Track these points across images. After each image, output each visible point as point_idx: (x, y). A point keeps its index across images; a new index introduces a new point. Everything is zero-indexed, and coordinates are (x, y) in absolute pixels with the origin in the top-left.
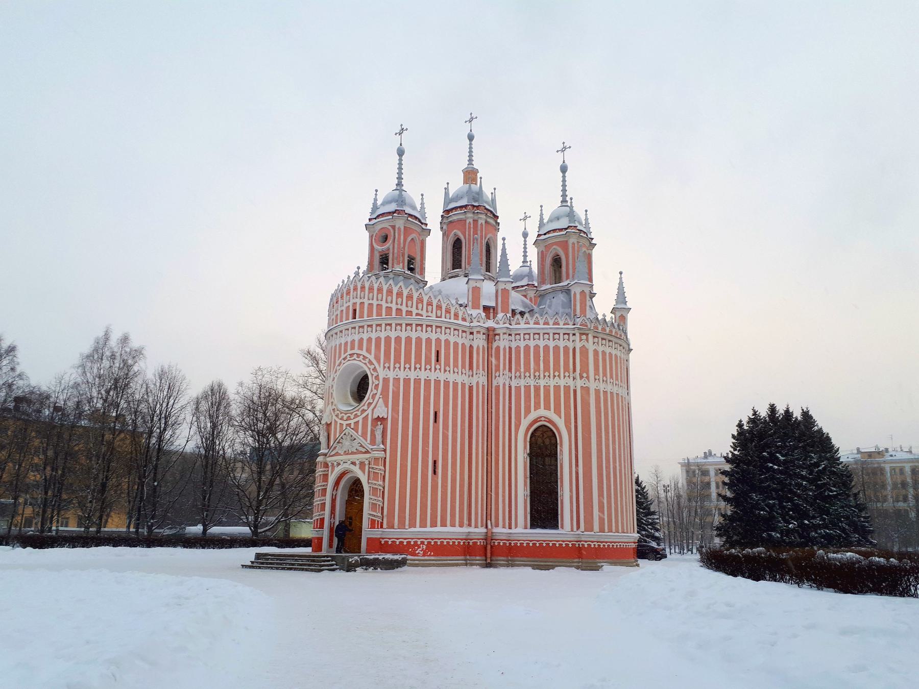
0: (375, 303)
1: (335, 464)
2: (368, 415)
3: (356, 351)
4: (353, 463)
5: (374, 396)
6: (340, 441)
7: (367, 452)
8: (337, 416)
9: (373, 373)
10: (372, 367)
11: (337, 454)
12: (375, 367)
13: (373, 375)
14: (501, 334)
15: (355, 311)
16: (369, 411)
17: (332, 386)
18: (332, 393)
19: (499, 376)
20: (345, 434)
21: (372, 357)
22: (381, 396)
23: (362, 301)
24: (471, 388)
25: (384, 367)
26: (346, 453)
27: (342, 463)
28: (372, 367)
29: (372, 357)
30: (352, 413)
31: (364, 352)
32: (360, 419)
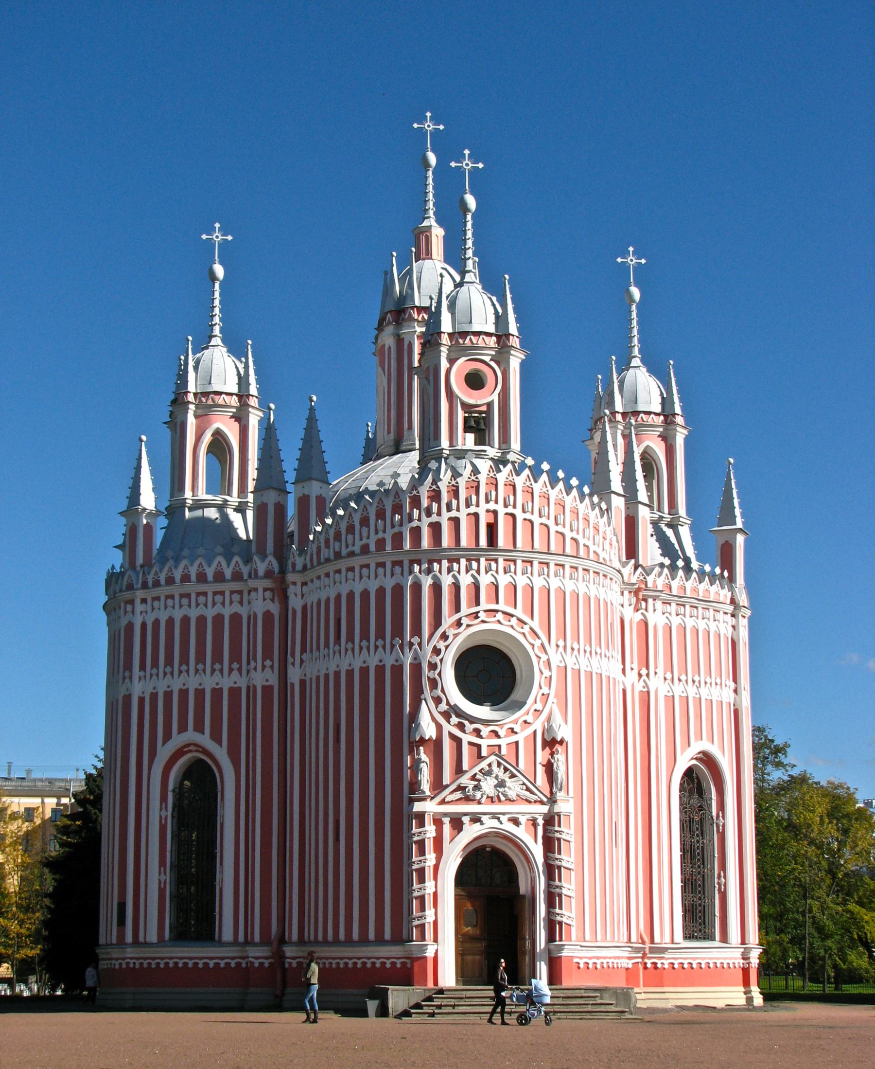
0: (537, 521)
1: (465, 819)
2: (535, 732)
3: (501, 606)
4: (516, 822)
5: (546, 697)
6: (478, 777)
7: (542, 803)
8: (461, 726)
9: (540, 654)
10: (537, 643)
11: (468, 799)
12: (542, 645)
13: (540, 658)
14: (650, 601)
15: (492, 528)
16: (538, 726)
17: (433, 666)
18: (434, 684)
19: (648, 675)
20: (490, 765)
21: (535, 625)
22: (555, 701)
23: (510, 510)
24: (624, 691)
25: (558, 646)
26: (491, 800)
27: (484, 818)
28: (537, 643)
29: (535, 625)
30: (501, 726)
31: (519, 612)
32: (520, 738)
